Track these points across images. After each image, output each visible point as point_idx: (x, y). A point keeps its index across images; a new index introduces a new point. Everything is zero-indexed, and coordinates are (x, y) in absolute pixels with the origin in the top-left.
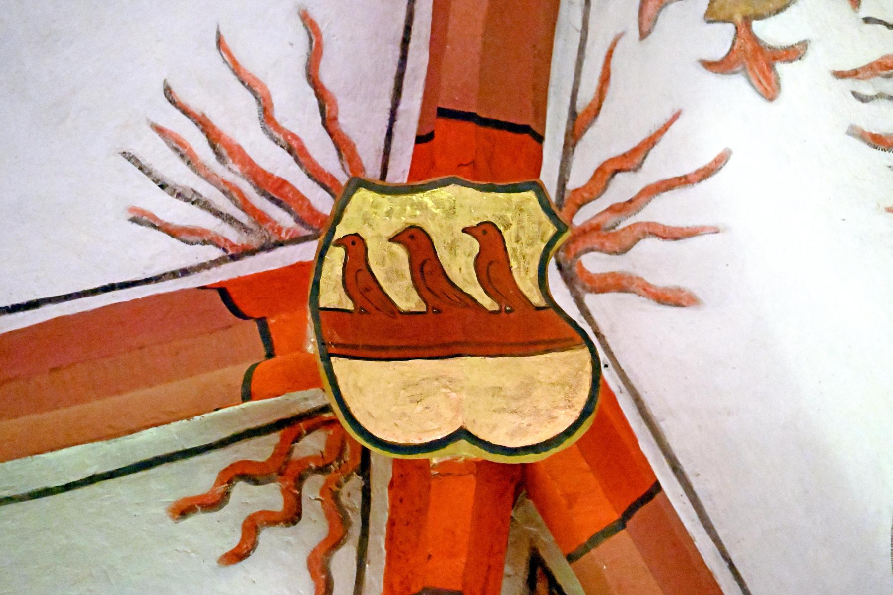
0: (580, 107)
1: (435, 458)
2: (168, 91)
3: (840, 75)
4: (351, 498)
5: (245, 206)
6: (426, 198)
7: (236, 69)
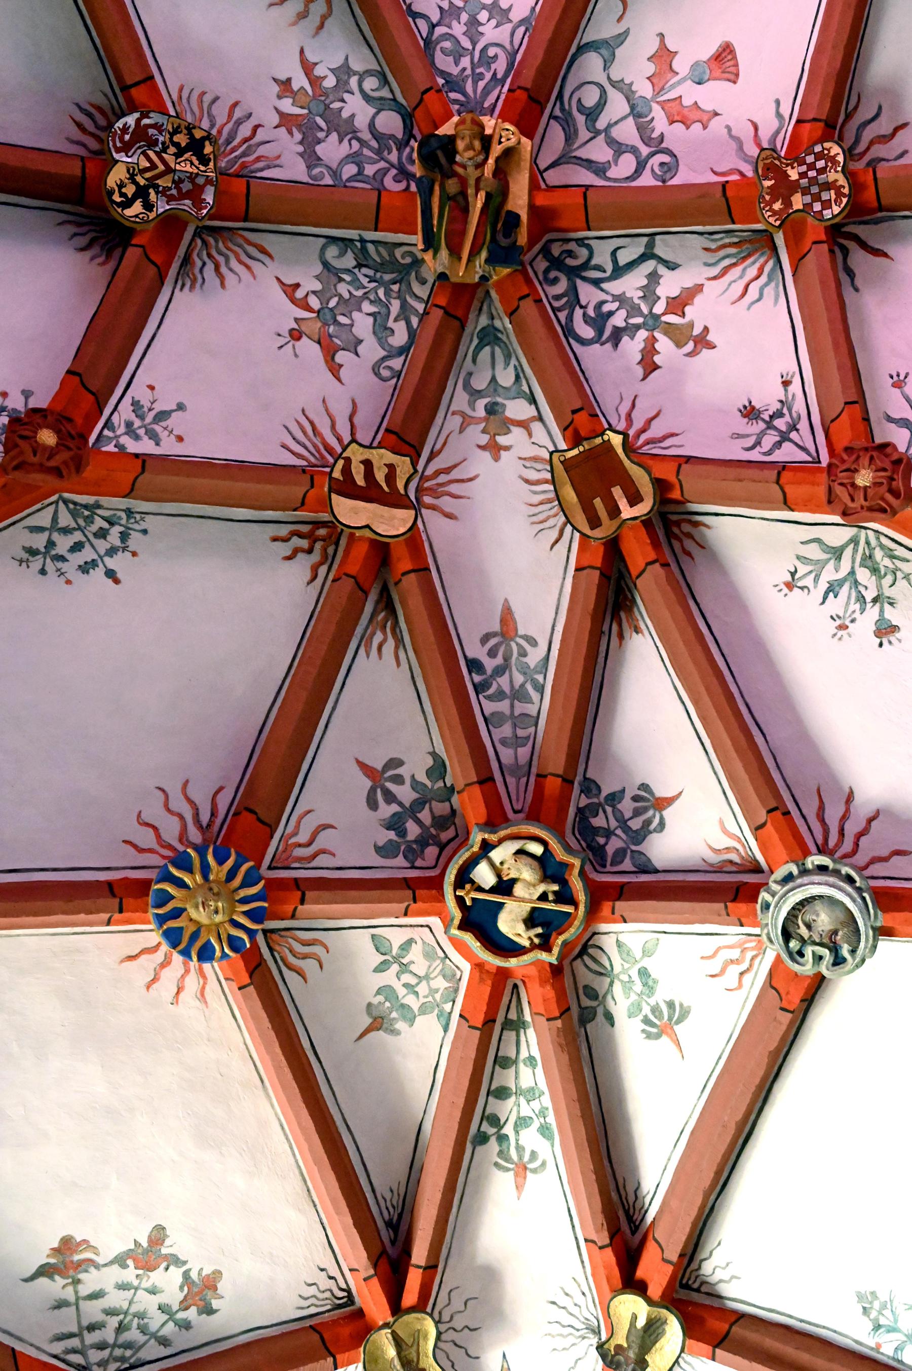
0: (435, 450)
1: (358, 533)
3: (520, 458)
4: (331, 550)
5: (319, 451)
7: (327, 410)
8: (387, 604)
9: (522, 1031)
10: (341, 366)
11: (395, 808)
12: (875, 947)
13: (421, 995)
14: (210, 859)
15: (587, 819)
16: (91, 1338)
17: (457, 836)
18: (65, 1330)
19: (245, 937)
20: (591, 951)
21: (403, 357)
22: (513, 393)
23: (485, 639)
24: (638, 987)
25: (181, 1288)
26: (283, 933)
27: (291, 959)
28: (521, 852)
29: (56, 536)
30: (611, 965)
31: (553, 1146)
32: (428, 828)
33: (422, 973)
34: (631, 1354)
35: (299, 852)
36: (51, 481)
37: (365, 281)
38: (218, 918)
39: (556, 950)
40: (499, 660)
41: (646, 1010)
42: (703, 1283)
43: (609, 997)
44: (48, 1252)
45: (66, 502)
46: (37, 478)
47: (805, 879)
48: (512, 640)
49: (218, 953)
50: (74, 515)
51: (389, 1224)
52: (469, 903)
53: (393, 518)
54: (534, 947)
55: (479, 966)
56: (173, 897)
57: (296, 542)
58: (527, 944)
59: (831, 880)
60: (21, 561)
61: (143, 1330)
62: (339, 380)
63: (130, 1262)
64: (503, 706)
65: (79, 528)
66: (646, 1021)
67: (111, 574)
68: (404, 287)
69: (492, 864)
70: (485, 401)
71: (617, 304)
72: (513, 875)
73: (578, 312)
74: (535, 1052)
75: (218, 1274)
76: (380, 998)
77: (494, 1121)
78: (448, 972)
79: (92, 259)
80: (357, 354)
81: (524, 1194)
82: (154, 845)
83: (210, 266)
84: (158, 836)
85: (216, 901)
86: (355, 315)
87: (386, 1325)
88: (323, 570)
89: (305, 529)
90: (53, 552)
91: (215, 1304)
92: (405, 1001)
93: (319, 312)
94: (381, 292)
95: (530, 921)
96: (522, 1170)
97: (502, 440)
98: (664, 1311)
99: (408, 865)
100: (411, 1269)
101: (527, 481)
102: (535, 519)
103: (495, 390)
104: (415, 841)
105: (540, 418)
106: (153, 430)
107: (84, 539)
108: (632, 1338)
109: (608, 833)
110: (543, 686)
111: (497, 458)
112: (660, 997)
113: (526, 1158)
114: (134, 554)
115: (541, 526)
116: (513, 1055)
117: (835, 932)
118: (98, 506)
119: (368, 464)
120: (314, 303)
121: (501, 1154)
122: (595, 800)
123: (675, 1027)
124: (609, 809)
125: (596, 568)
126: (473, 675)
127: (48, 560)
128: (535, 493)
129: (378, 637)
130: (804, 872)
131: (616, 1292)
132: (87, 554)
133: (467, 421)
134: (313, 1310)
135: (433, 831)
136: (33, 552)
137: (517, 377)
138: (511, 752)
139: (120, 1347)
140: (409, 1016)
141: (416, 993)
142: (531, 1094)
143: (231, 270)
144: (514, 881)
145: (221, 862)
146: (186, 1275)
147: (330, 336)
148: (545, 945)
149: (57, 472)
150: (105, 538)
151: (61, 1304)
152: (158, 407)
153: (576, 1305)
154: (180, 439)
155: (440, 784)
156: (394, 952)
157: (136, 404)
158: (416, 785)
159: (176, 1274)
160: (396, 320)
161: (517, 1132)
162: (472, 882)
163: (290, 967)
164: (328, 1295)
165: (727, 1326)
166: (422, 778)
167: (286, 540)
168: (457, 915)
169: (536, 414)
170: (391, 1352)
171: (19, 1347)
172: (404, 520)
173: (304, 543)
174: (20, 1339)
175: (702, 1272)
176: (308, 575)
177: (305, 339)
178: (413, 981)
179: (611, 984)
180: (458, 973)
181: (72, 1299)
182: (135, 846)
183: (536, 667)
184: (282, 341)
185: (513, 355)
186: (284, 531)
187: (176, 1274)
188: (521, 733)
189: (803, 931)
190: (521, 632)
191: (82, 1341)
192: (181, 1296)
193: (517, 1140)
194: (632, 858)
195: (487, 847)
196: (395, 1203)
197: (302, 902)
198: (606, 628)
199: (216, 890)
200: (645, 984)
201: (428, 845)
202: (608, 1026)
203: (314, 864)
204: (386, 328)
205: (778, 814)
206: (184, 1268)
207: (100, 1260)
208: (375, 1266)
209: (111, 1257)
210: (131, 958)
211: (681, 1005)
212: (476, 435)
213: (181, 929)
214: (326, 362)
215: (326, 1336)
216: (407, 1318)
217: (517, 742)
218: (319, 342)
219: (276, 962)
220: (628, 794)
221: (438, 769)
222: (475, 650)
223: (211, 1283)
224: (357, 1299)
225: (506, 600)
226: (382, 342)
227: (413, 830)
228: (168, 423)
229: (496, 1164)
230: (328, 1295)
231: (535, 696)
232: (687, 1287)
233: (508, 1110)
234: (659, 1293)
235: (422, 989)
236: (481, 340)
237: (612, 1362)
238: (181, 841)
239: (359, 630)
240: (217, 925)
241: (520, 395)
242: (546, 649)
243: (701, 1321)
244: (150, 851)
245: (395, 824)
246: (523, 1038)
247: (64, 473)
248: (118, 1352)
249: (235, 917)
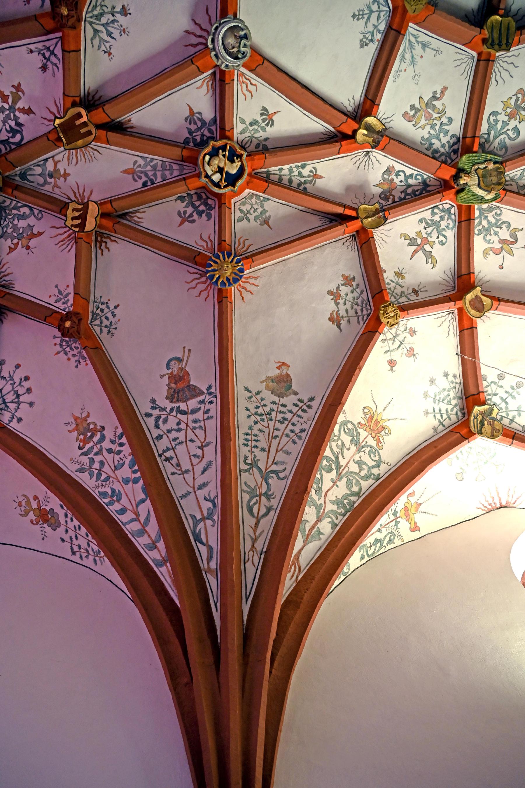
0: (67, 198)
1: (98, 223)
2: (55, 245)
3: (68, 165)
4: (105, 236)
5: (70, 239)
6: (68, 216)
8: (124, 216)
9: (270, 172)
10: (38, 232)
11: (195, 214)
12: (241, 20)
13: (257, 207)
14: (210, 269)
15: (198, 143)
16: (359, 313)
17: (204, 192)
18: (356, 320)
19: (236, 258)
20: (243, 145)
21: (34, 209)
22: (44, 167)
23: (135, 180)
24: (256, 127)
25: (346, 286)
26: (236, 251)
27: (245, 249)
28: (209, 164)
29: (103, 325)
30: (248, 137)
31: (308, 164)
32: (202, 203)
33: (250, 206)
34: (375, 136)
35: (209, 245)
36: (83, 322)
37: (6, 223)
38: (230, 266)
39: (242, 152)
40: (142, 175)
41: (264, 124)
42: (354, 111)
43: (259, 139)
44: (333, 325)
45: (91, 322)
46: (82, 327)
47: (217, 48)
48: (135, 170)
49: (241, 267)
50: (96, 319)
51: (331, 222)
52: (226, 184)
53: (92, 210)
54: (241, 161)
55: (248, 185)
56: (223, 281)
57: (103, 247)
58: (240, 163)
59: (216, 36)
60: (112, 335)
61: (358, 298)
62: (44, 232)
63: (338, 301)
64: (159, 174)
65: (100, 318)
66: (267, 125)
67: (116, 307)
68: (7, 209)
69: (213, 175)
70: (48, 178)
71: (6, 124)
72: (217, 167)
73: (11, 140)
74: (277, 168)
75: (343, 276)
76: (258, 221)
77: (299, 184)
78: (250, 198)
79: (5, 318)
80: (34, 226)
81: (324, 176)
82: (207, 292)
83: (5, 278)
84: (204, 290)
85: (224, 267)
86: (19, 226)
87: (361, 221)
88: (113, 238)
89: (98, 244)
90: (109, 326)
91: (352, 277)
92: (259, 213)
93: (19, 239)
94: (10, 217)
95: (232, 161)
96: (316, 176)
97: (62, 172)
98: (363, 123)
99: (214, 210)
100: (345, 213)
101: (77, 163)
102: (91, 161)
103: (43, 174)
104: (206, 207)
105: (53, 157)
106: (65, 295)
107: (104, 316)
108: (370, 136)
109: (203, 135)
110: (151, 159)
111: (69, 175)
112: (259, 118)
113: (312, 174)
114: (109, 300)
115: (93, 158)
116: (278, 177)
117: (235, 36)
118: (93, 312)
119: (73, 219)
120: (16, 241)
121: (310, 183)
122: (191, 139)
123: (270, 113)
124: (194, 134)
125: (107, 133)
126: (148, 185)
127: (112, 327)
128: (81, 160)
129: (135, 219)
130: (214, 49)
131: (356, 141)
132: (109, 315)
133: (56, 186)
134: (356, 247)
135: (202, 201)
136: (109, 332)
137: (38, 166)
138: (175, 171)
139: (363, 305)
140: (264, 211)
141: (257, 209)
142: (291, 170)
143: (6, 271)
144: (219, 167)
145: (211, 266)
146: (342, 285)
147: (28, 235)
148: (240, 156)
149: (80, 320)
150: (103, 310)
151: (349, 322)
152: (57, 294)
153: (359, 160)
154: (68, 286)
155: (186, 198)
156: (243, 215)
157: (56, 301)
158: (186, 207)
159: (342, 288)
160: (20, 212)
161: (303, 177)
162: (219, 182)
163: (247, 249)
164: (351, 242)
165: (369, 101)
166: (184, 204)
167: (102, 251)
168: (230, 188)
169: (51, 159)
170: (370, 219)
171: (361, 333)
172: (93, 205)
173: (103, 244)
174: (358, 333)
175: (351, 111)
176: (115, 243)
177: (29, 244)
178: (253, 209)
179: (255, 137)
180: (250, 194)
181: (347, 318)
182: (207, 298)
183: (144, 161)
184: (30, 252)
185: (30, 167)
186: (99, 252)
187: (342, 288)
188: (168, 168)
189: (235, 50)
190: (132, 167)
191: (360, 316)
192: (349, 287)
193: (306, 177)
194: (211, 126)
195: (207, 176)
196: (324, 220)
197: (225, 241)
198: (129, 133)
199: (220, 267)
200: (255, 124)
201: (207, 202)
202: (269, 140)
203: (213, 241)
204: (23, 215)
205: (194, 60)
206: (341, 285)
207: (336, 310)
208: (342, 224)
209: (335, 307)
210: (243, 299)
211: (262, 110)
212: (61, 182)
213: (233, 278)
214: (37, 237)
215: (364, 242)
216: (360, 215)
217: (171, 169)
218: (30, 239)
219: (245, 254)
220: (188, 126)
221: (181, 199)
222: (139, 184)
223: (345, 278)
224: (353, 233)
225: (121, 172)
226: (28, 217)
227: (202, 208)
228: (62, 290)
229: (313, 185)
230: (351, 242)
231: (155, 162)
232: (355, 117)
233: (296, 180)
234: (356, 124)
235: (255, 206)
236: (25, 180)
237: (377, 144)
238: (205, 283)
239: (133, 225)
240: (232, 267)
241: (44, 164)
242: (138, 157)
243: (366, 111)
244: (208, 293)
245: (200, 213)
246: (273, 172)
247: (80, 318)
248: (364, 306)
249: (230, 261)
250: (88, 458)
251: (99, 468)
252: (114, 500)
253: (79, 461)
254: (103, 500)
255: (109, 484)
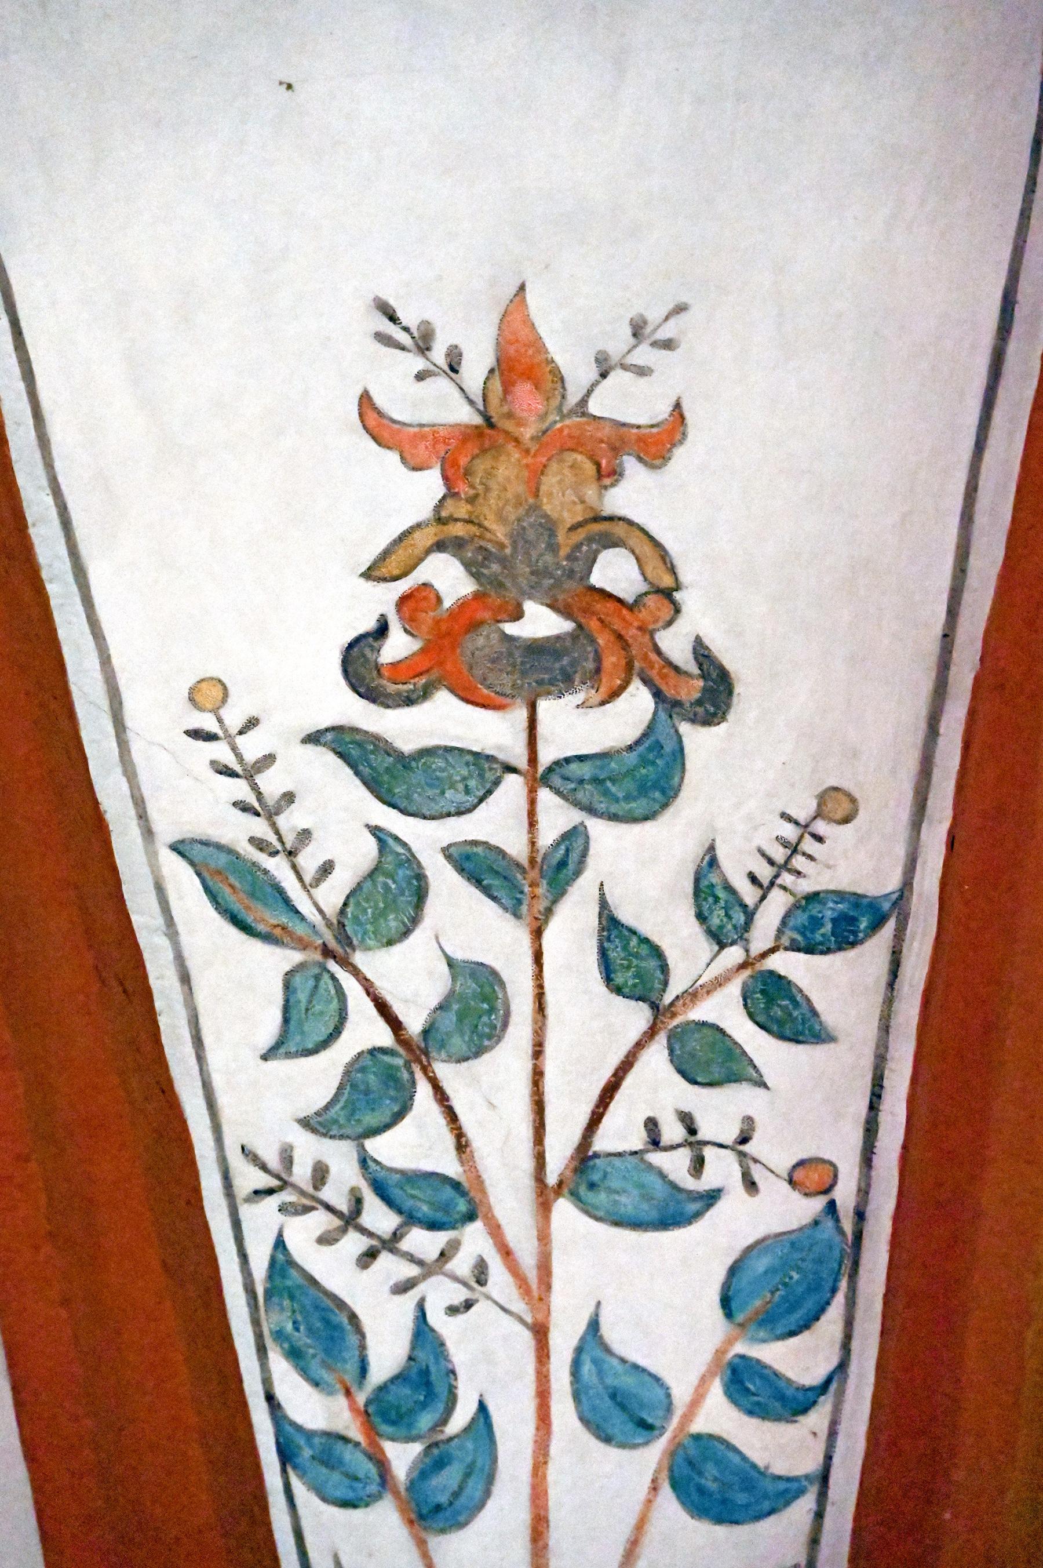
250: (376, 831)
251: (414, 1024)
252: (382, 1465)
253: (272, 783)
254: (279, 1365)
255: (430, 1269)
